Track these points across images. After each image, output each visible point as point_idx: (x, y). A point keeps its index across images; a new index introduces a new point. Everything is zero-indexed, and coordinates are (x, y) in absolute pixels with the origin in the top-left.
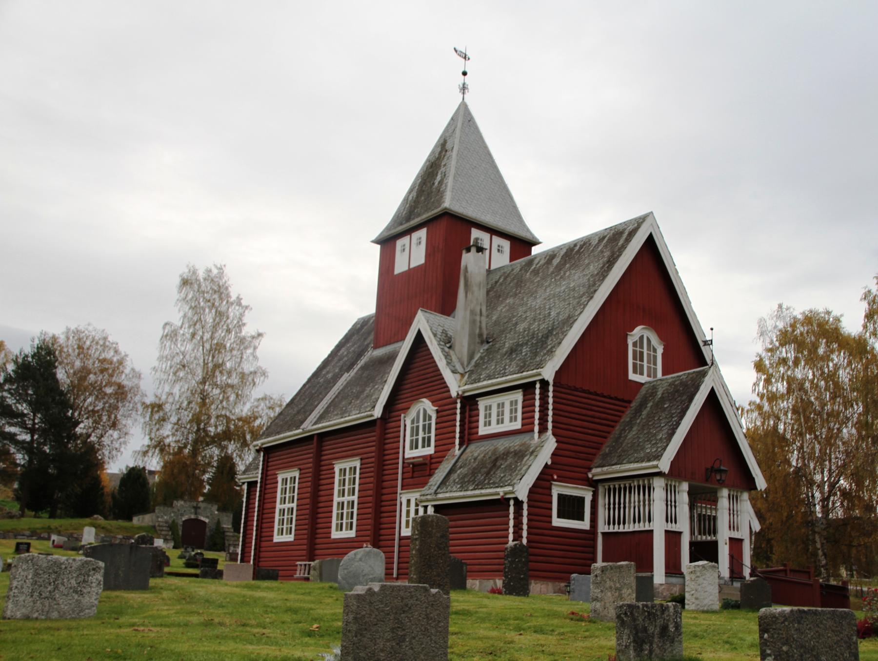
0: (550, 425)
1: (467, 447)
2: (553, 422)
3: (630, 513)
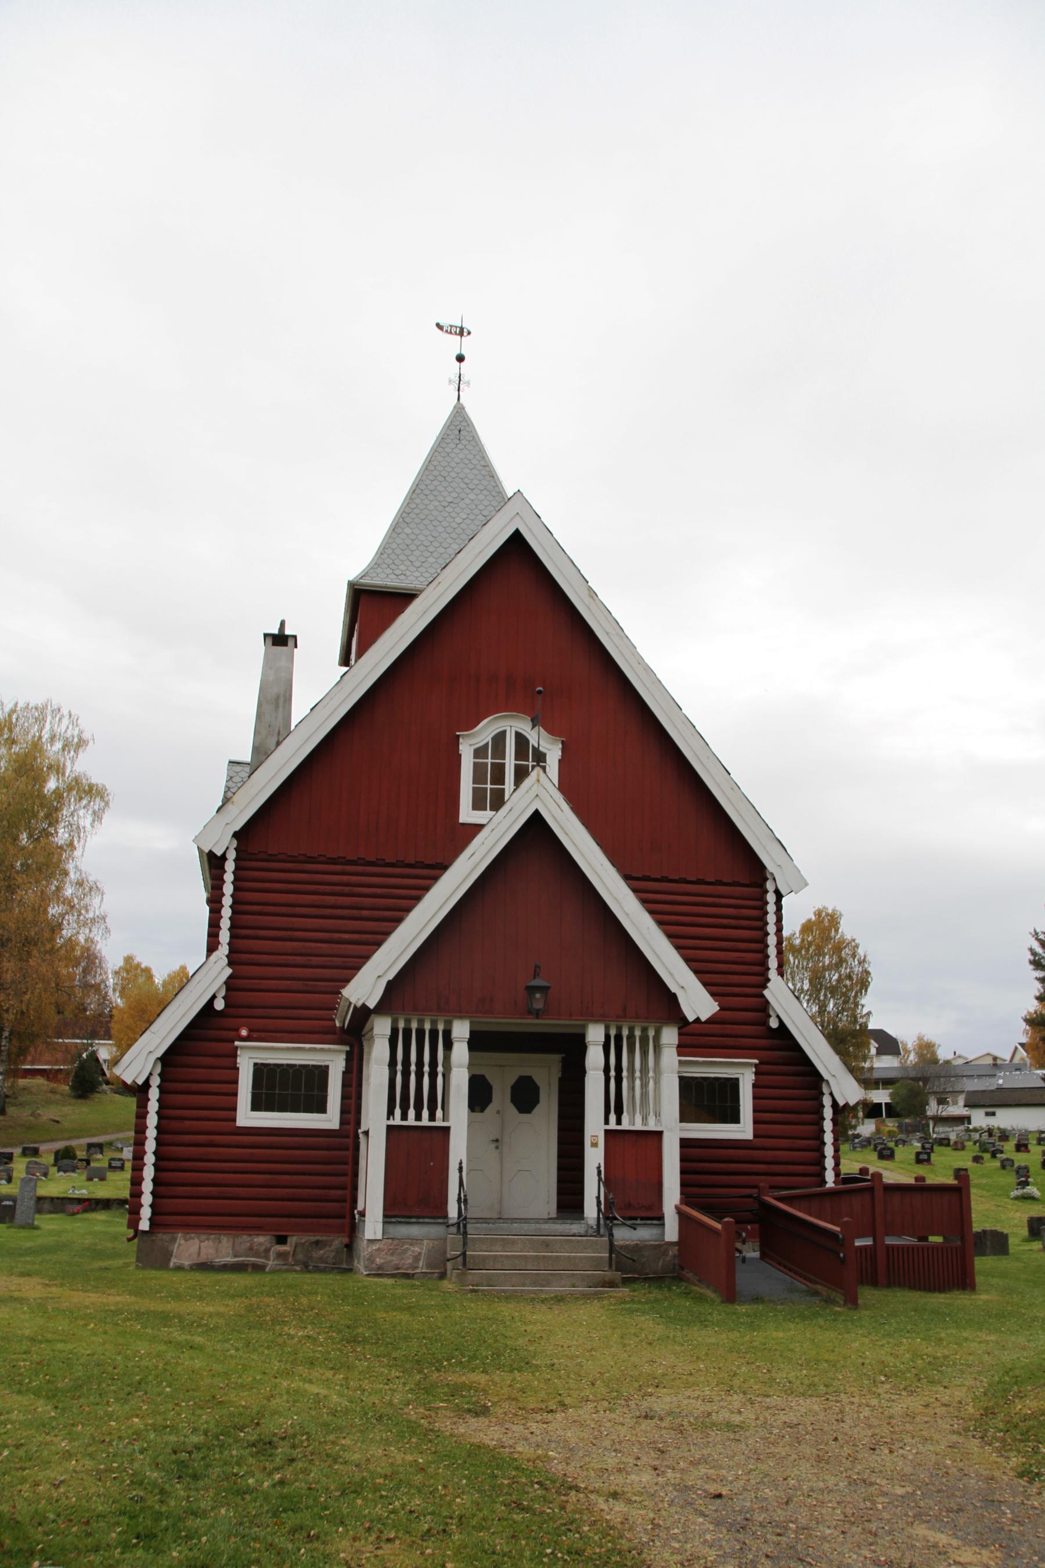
0: (224, 936)
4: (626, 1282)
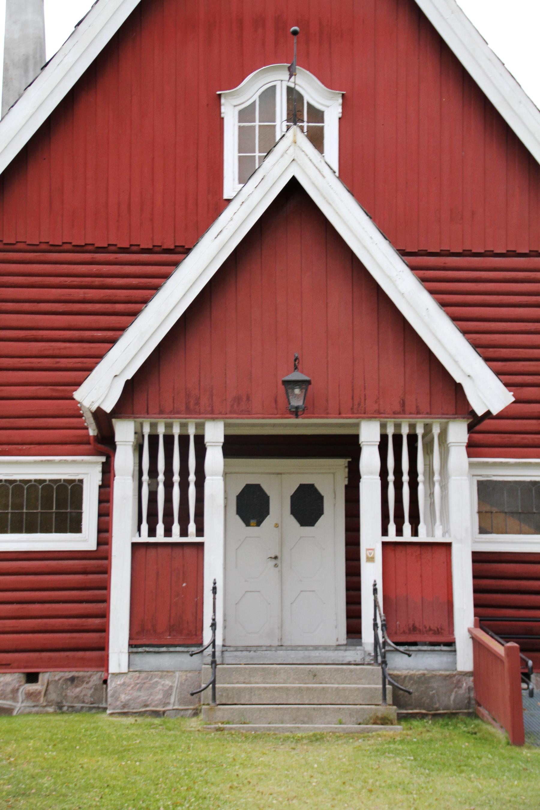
4: (401, 718)
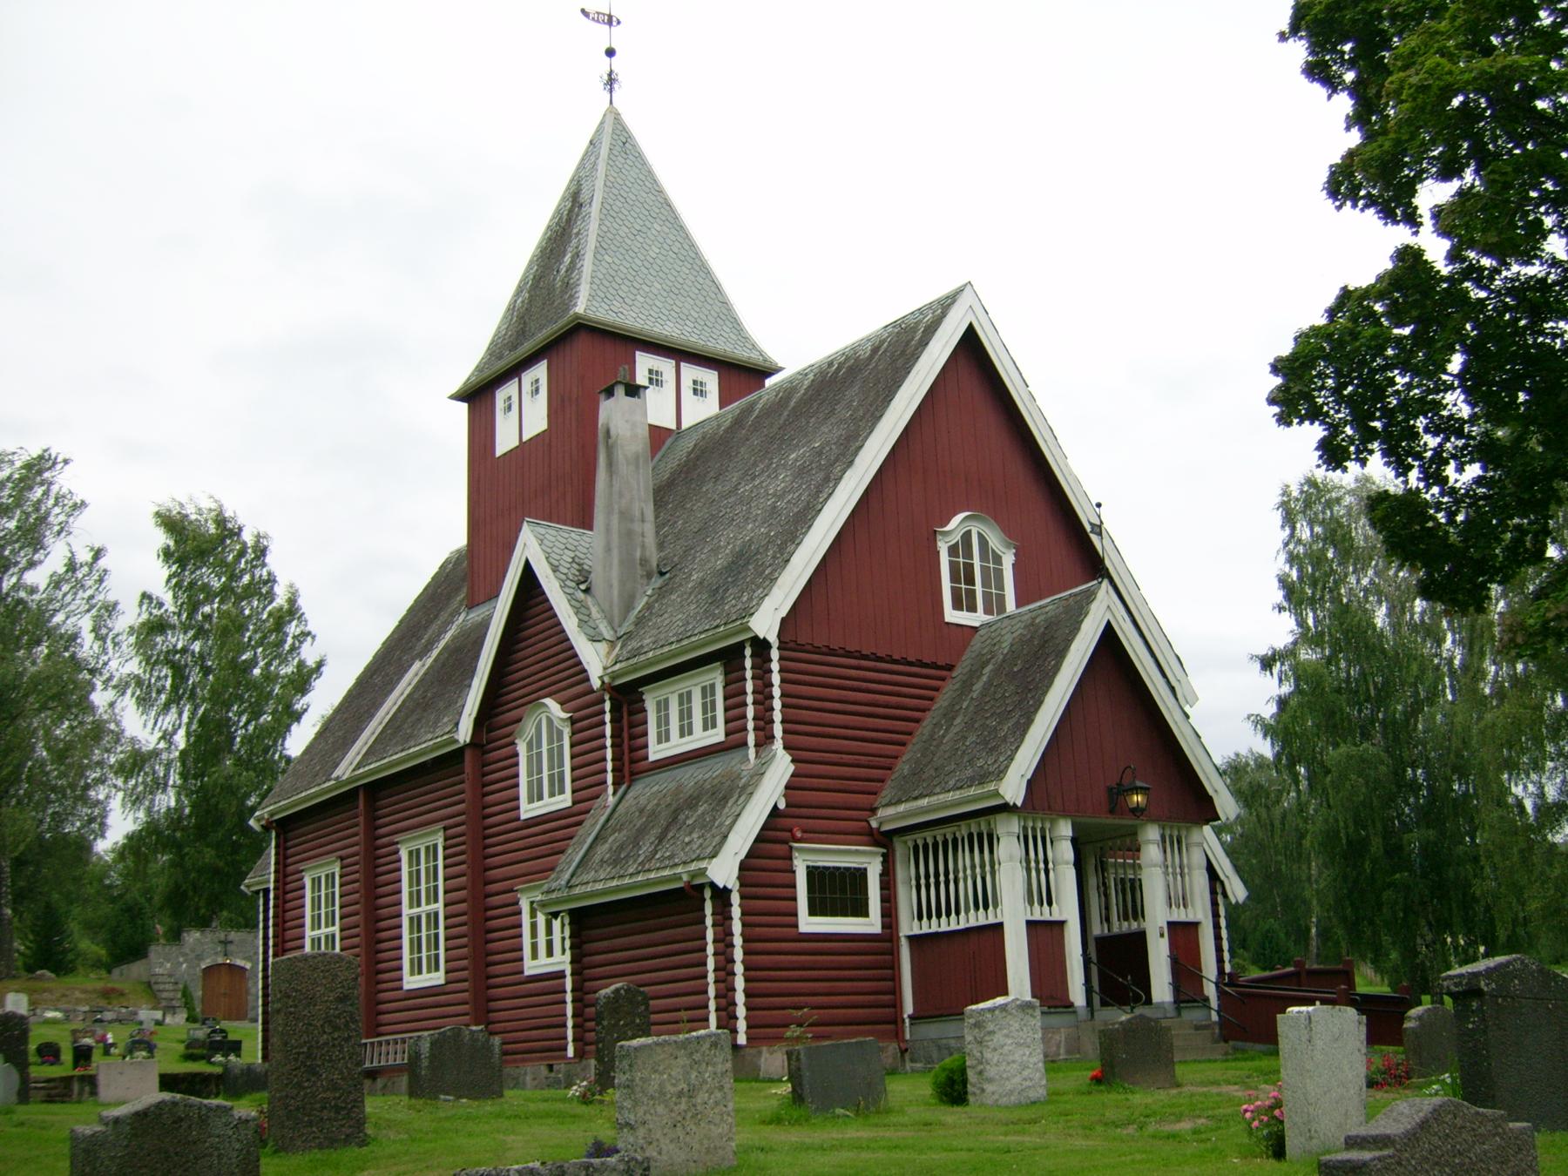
0: (778, 730)
1: (629, 787)
2: (783, 722)
3: (966, 889)
